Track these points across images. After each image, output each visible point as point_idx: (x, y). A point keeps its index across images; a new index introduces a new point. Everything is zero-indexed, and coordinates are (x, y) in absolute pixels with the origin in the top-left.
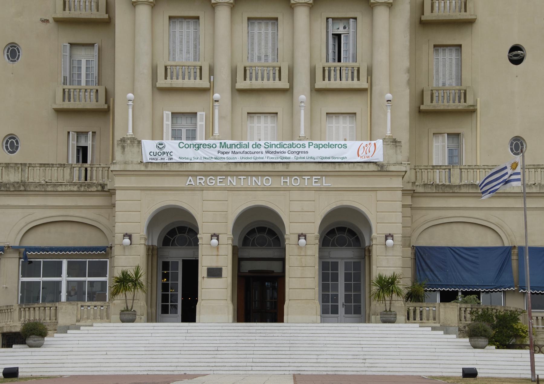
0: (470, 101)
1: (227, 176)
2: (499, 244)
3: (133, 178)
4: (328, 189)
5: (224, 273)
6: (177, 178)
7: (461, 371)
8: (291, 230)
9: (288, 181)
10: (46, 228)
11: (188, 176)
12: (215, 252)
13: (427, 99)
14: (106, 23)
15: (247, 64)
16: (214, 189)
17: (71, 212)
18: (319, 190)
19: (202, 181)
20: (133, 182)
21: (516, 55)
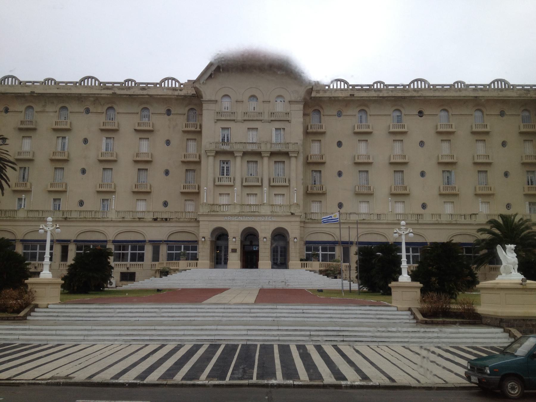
0: (324, 190)
2: (334, 240)
4: (274, 221)
8: (261, 235)
10: (176, 234)
12: (234, 242)
13: (309, 189)
14: (199, 163)
15: (247, 177)
16: (234, 221)
17: (185, 228)
20: (206, 218)
21: (340, 174)
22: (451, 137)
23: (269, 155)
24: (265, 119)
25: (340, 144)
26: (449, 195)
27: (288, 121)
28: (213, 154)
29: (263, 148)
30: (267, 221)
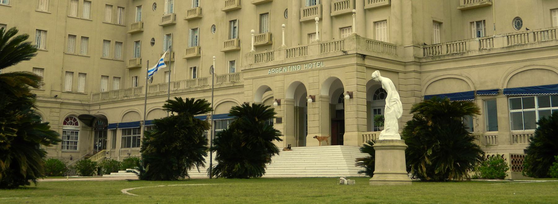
1: (283, 67)
3: (250, 73)
5: (283, 121)
6: (257, 72)
16: (279, 75)
18: (320, 70)
20: (247, 75)
30: (316, 70)
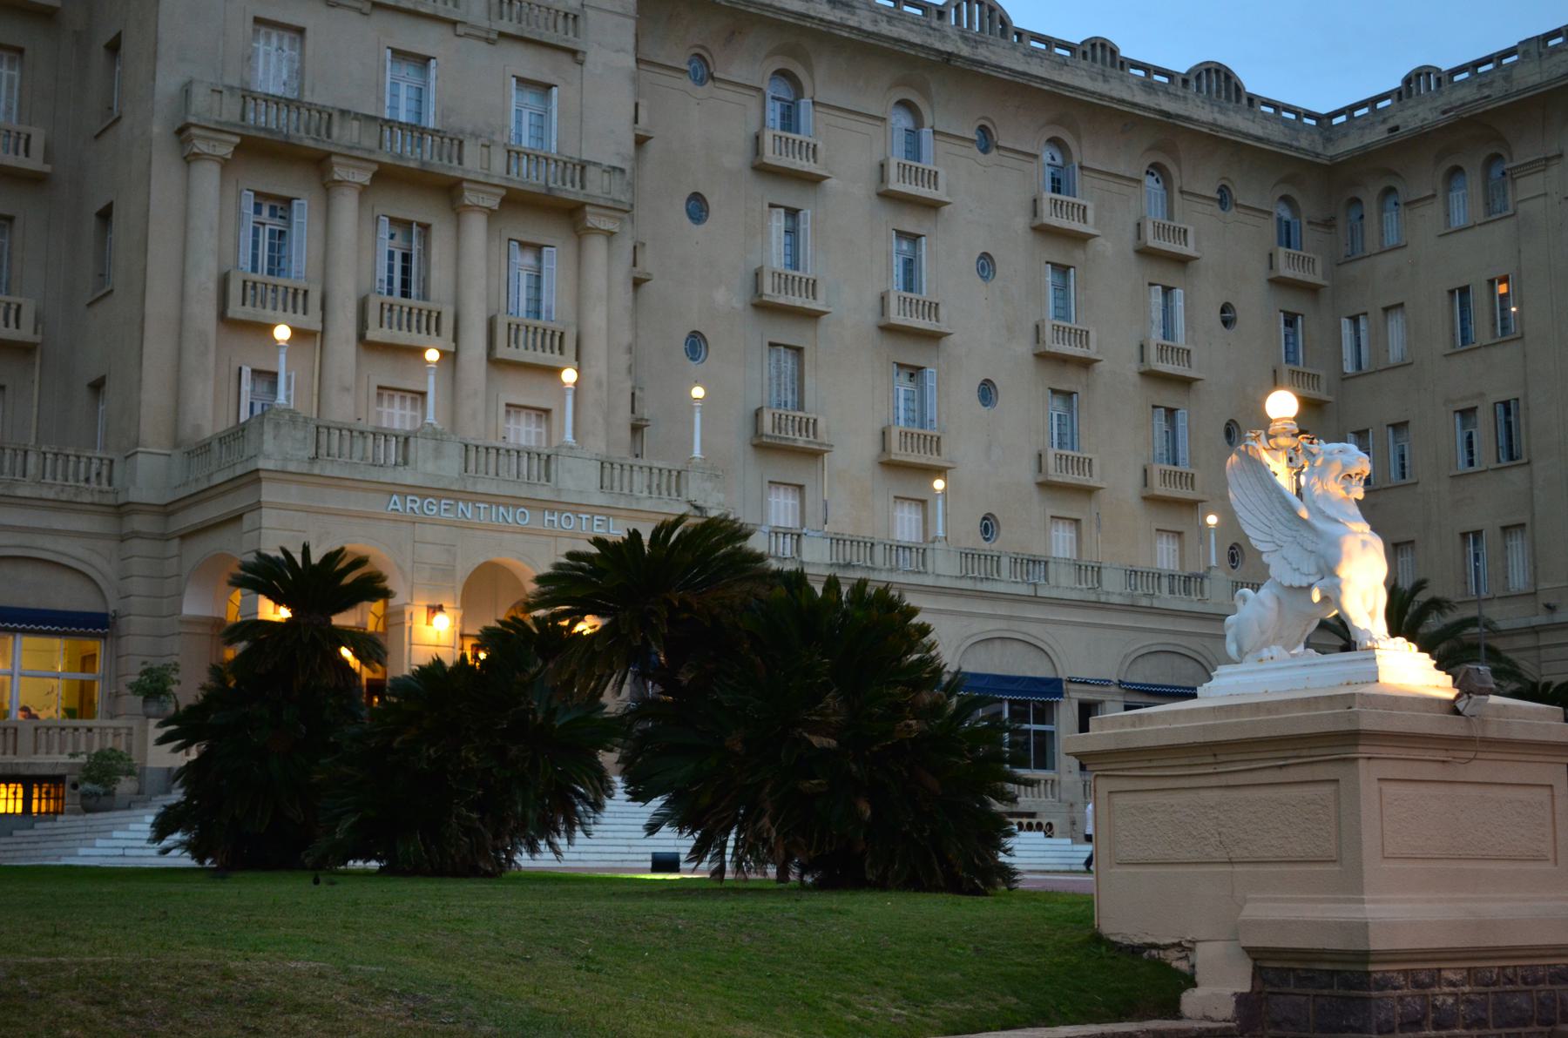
1: (457, 500)
7: (650, 857)
9: (555, 518)
11: (392, 494)
17: (40, 541)
19: (415, 506)
22: (1075, 256)
23: (493, 203)
24: (470, 19)
25: (698, 207)
26: (1067, 492)
27: (573, 53)
28: (226, 151)
29: (473, 163)
